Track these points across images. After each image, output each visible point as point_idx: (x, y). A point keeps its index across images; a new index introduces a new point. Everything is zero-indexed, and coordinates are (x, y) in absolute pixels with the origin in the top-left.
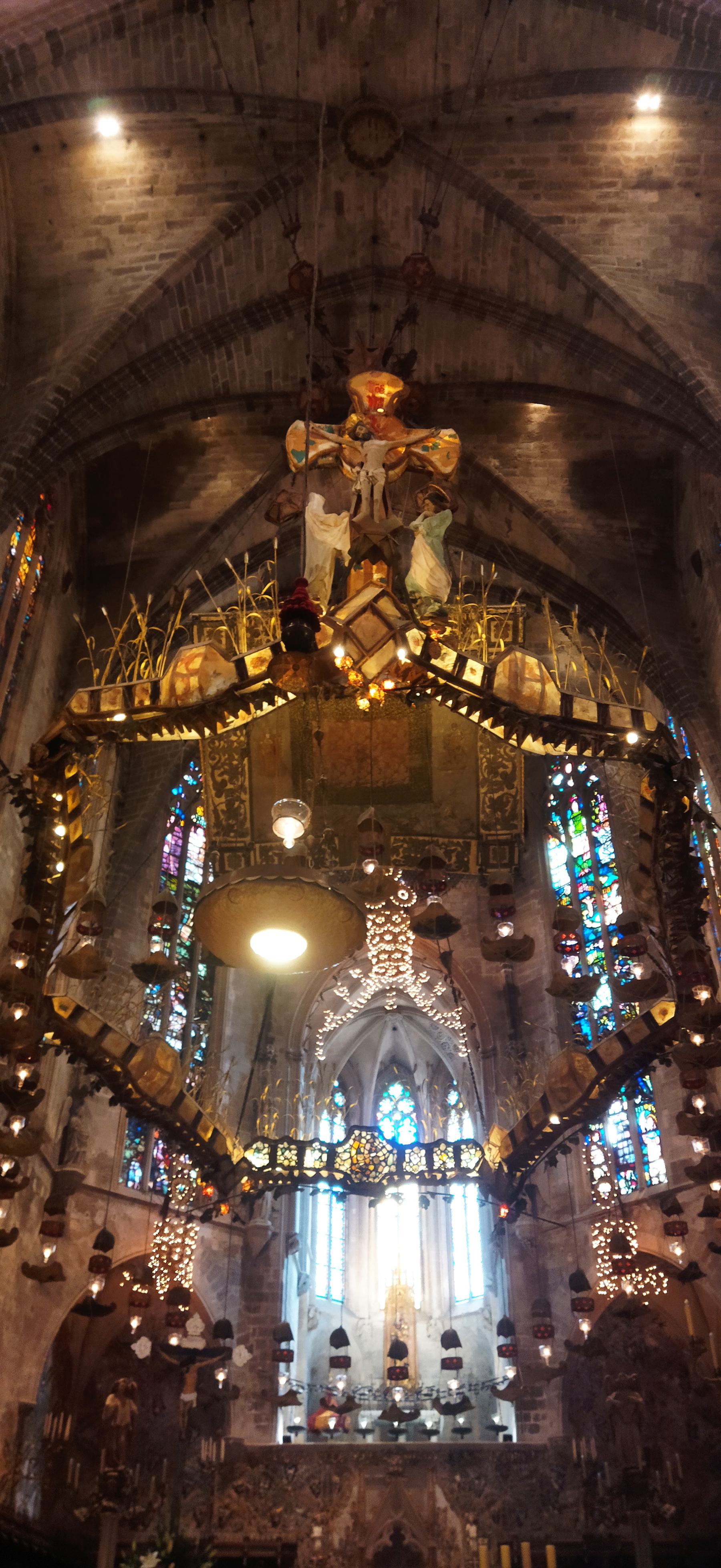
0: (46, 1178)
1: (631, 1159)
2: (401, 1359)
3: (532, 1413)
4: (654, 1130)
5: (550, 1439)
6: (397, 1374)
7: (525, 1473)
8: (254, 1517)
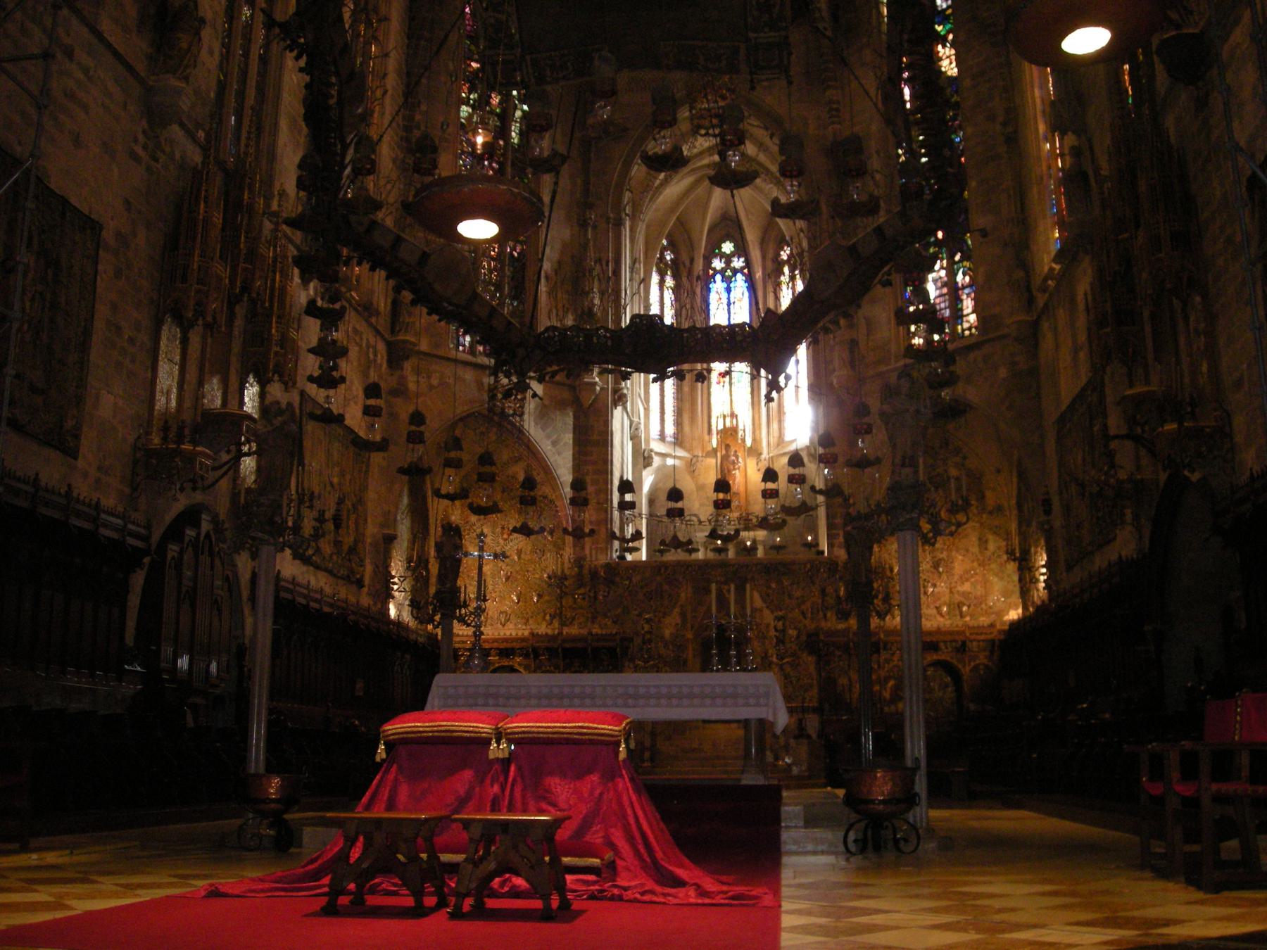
0: (381, 347)
2: (677, 501)
6: (721, 505)
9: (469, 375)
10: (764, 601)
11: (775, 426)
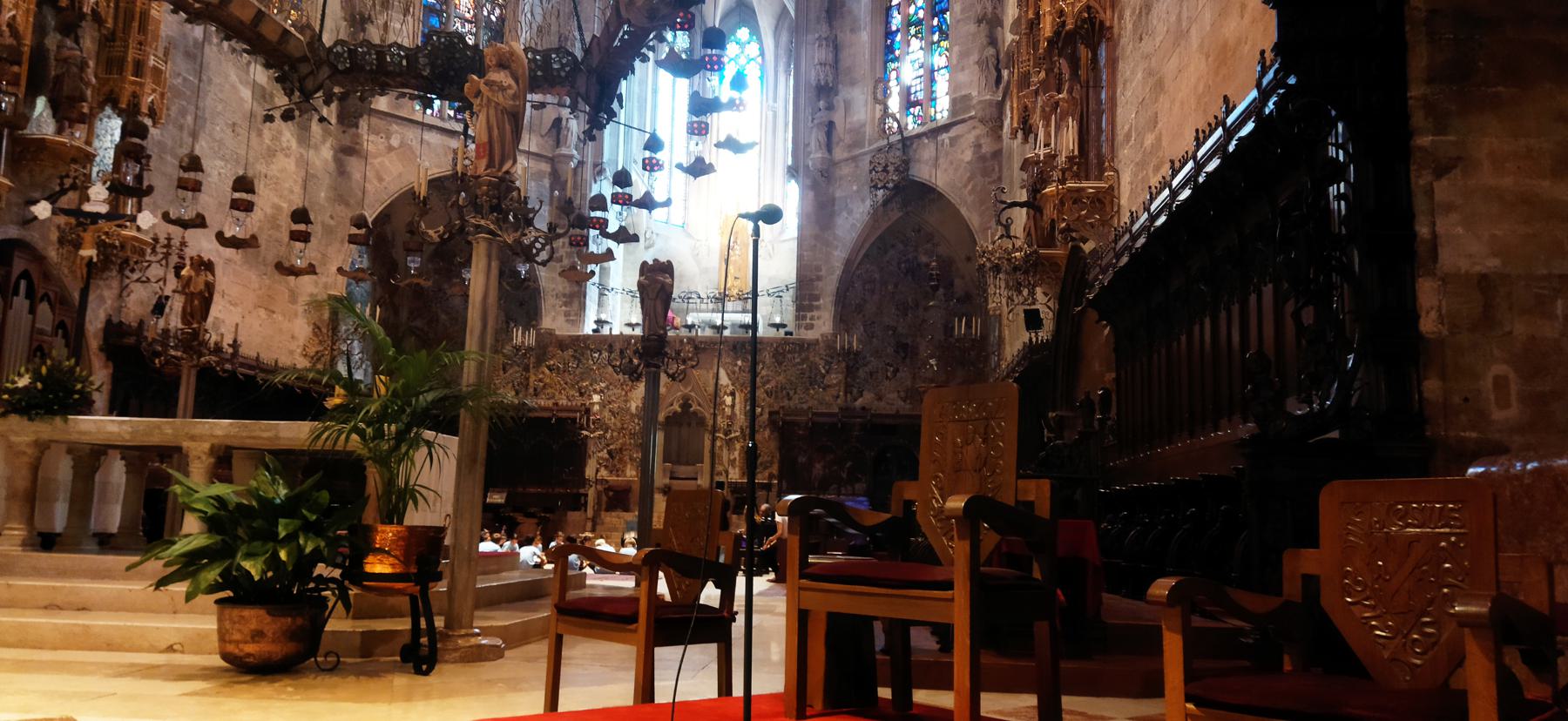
1: (920, 96)
3: (809, 315)
4: (946, 67)
5: (822, 335)
7: (798, 360)
8: (564, 389)
9: (432, 138)
10: (730, 379)
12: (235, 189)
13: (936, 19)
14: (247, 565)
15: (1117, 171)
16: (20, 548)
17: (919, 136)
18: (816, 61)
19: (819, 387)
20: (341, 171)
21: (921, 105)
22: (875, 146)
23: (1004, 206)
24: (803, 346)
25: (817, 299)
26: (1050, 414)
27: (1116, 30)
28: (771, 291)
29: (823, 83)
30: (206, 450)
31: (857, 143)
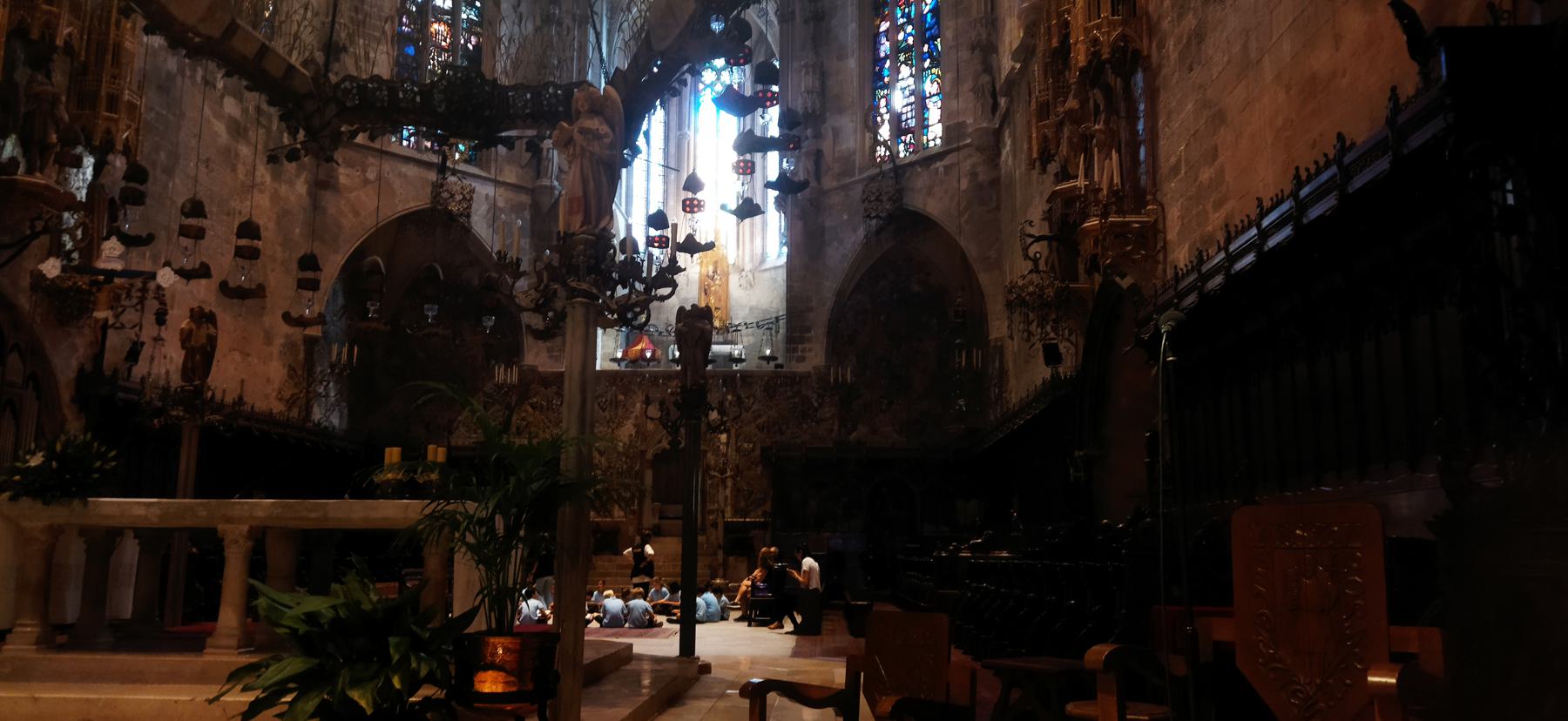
1: (912, 123)
3: (800, 347)
4: (937, 94)
5: (814, 368)
7: (789, 394)
8: (548, 427)
9: (411, 170)
11: (758, 241)
12: (239, 235)
13: (926, 46)
14: (355, 695)
15: (1162, 205)
16: (34, 647)
17: (912, 164)
18: (803, 89)
19: (812, 421)
20: (316, 206)
21: (913, 133)
22: (865, 175)
23: (1033, 239)
24: (795, 380)
25: (809, 330)
26: (1076, 453)
27: (1155, 59)
28: (760, 324)
29: (810, 111)
30: (244, 533)
31: (847, 170)
